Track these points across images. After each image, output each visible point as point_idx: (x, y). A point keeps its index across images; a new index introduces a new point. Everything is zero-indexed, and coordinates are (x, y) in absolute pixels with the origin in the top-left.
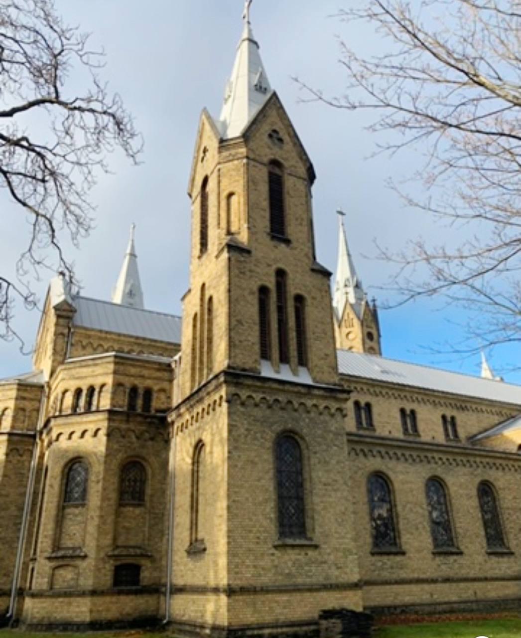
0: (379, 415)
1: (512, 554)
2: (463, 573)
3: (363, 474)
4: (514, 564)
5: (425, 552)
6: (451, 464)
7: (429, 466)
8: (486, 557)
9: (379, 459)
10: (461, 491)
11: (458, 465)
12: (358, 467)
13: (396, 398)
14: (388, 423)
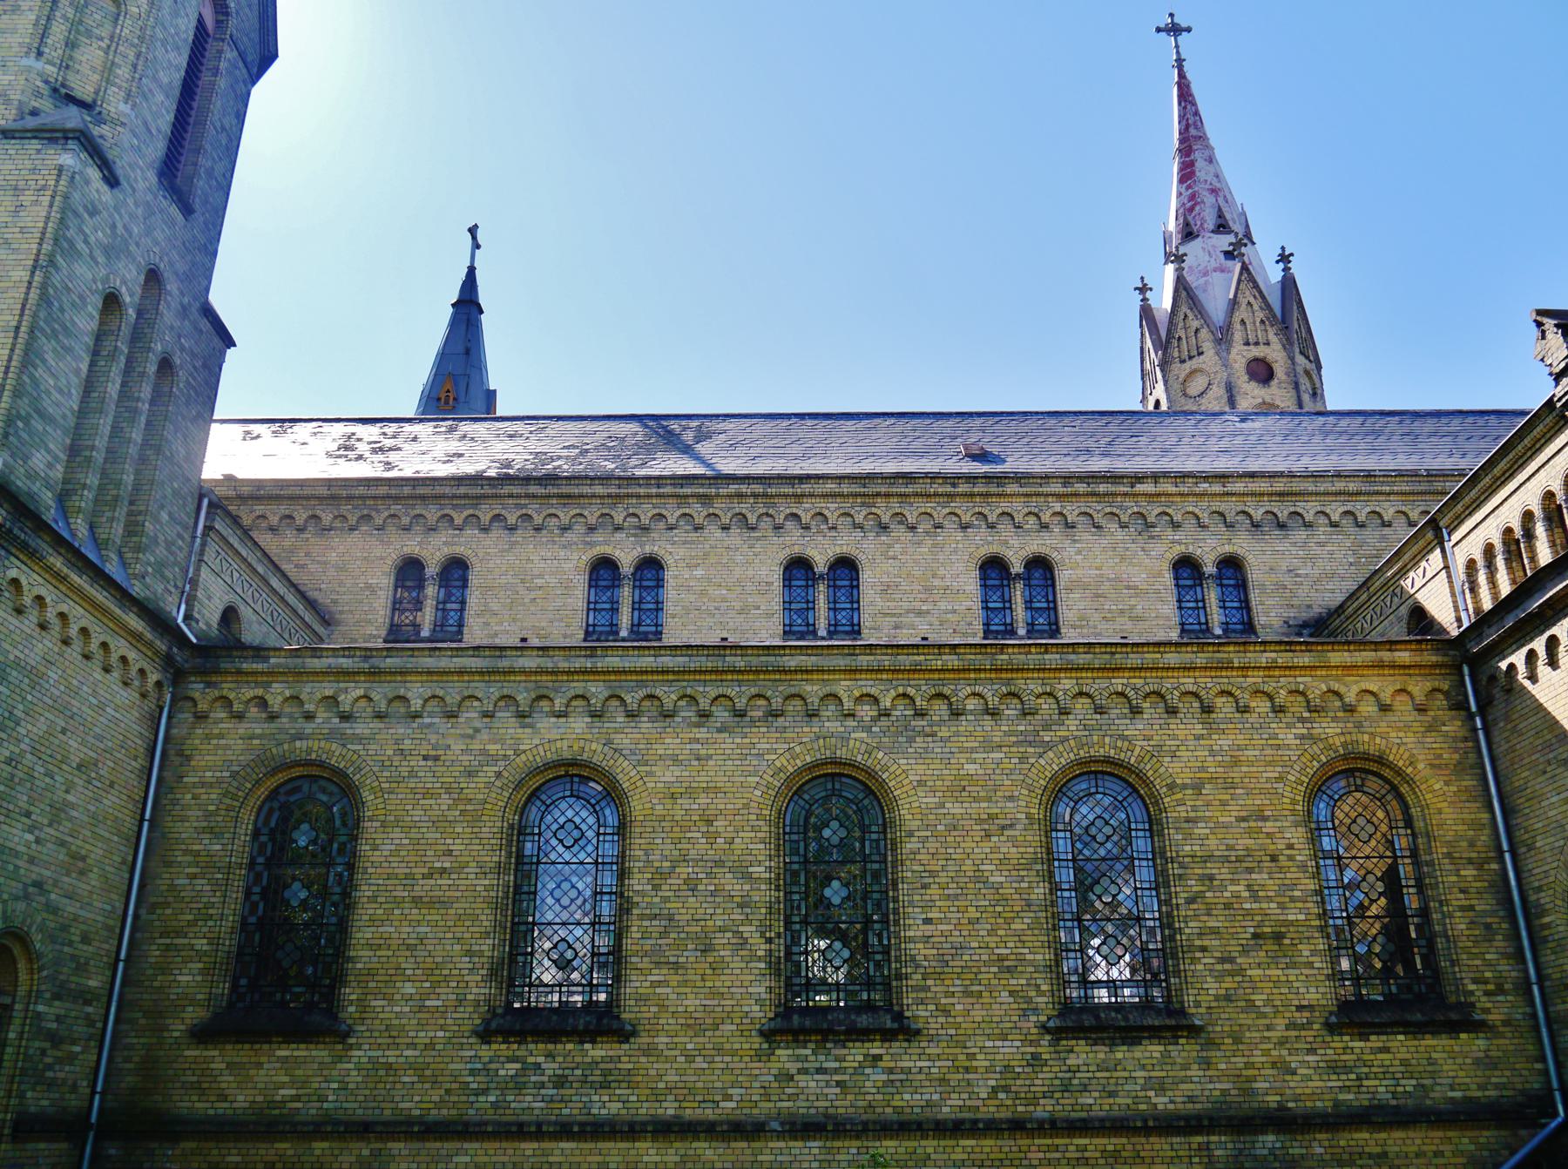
0: (886, 590)
1: (1194, 1031)
2: (910, 1101)
3: (499, 775)
4: (1195, 1072)
5: (728, 1028)
6: (920, 714)
7: (808, 731)
8: (1045, 1049)
9: (579, 724)
10: (956, 809)
11: (956, 713)
12: (484, 752)
13: (965, 527)
14: (920, 613)
